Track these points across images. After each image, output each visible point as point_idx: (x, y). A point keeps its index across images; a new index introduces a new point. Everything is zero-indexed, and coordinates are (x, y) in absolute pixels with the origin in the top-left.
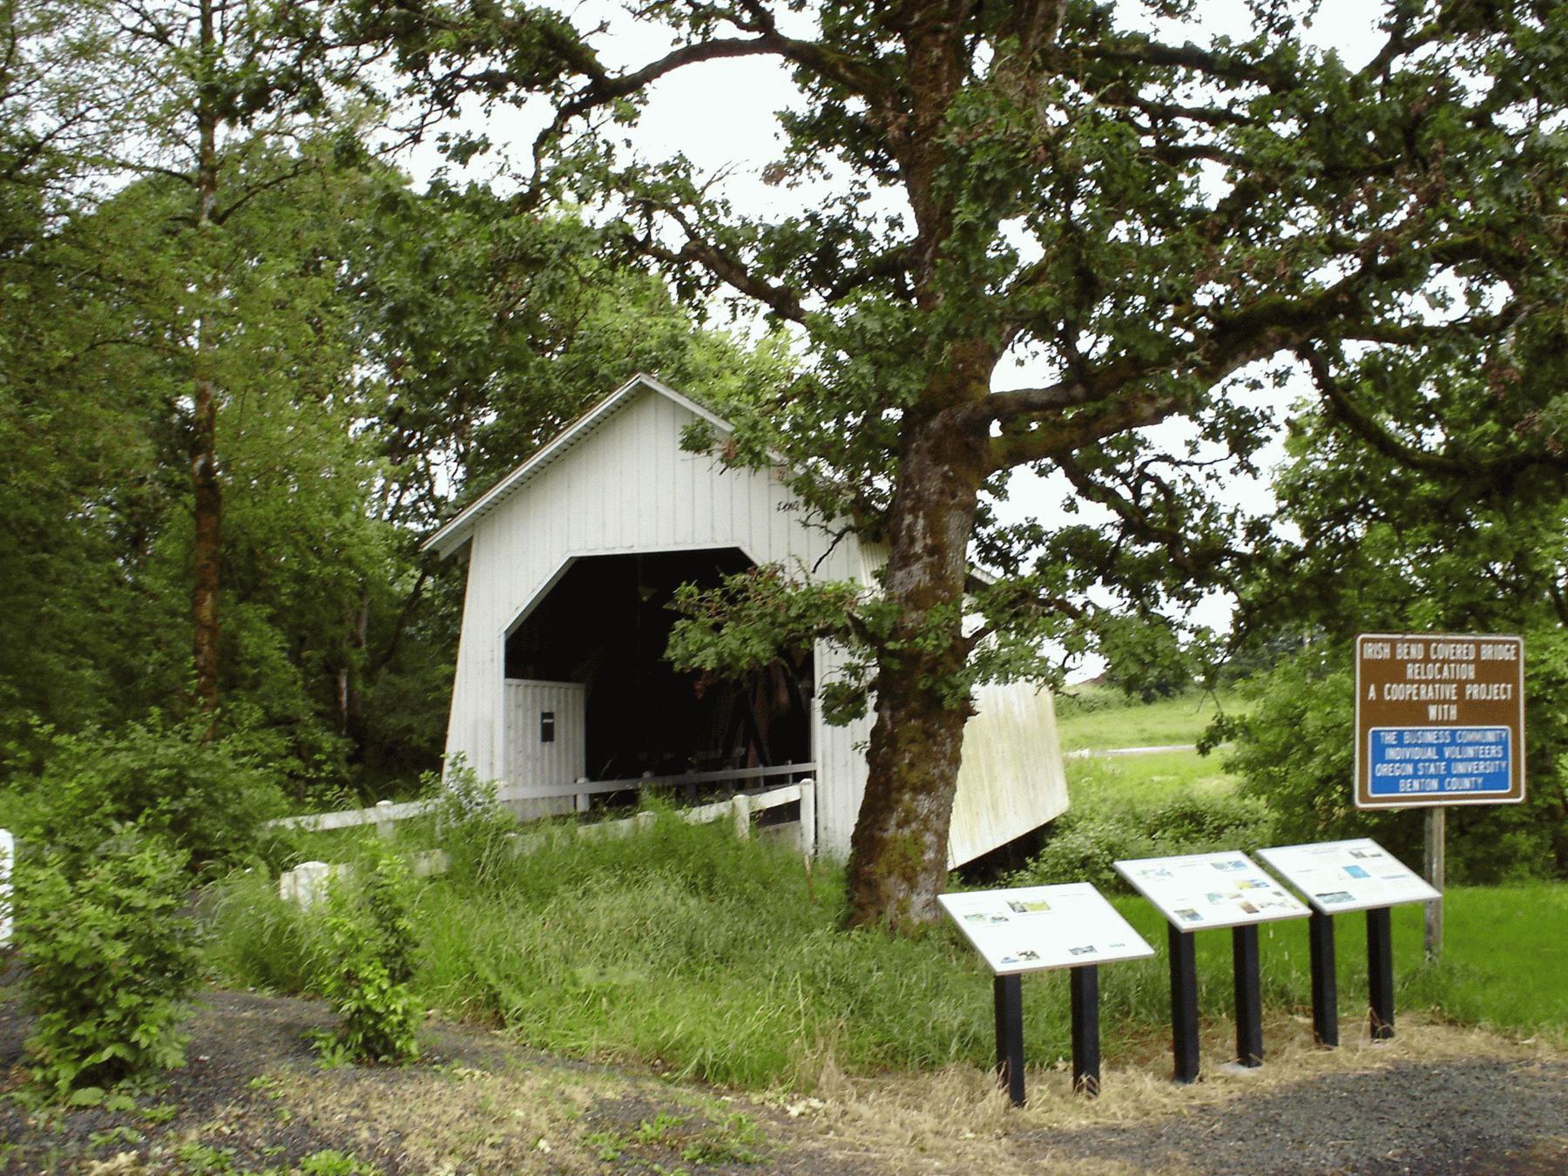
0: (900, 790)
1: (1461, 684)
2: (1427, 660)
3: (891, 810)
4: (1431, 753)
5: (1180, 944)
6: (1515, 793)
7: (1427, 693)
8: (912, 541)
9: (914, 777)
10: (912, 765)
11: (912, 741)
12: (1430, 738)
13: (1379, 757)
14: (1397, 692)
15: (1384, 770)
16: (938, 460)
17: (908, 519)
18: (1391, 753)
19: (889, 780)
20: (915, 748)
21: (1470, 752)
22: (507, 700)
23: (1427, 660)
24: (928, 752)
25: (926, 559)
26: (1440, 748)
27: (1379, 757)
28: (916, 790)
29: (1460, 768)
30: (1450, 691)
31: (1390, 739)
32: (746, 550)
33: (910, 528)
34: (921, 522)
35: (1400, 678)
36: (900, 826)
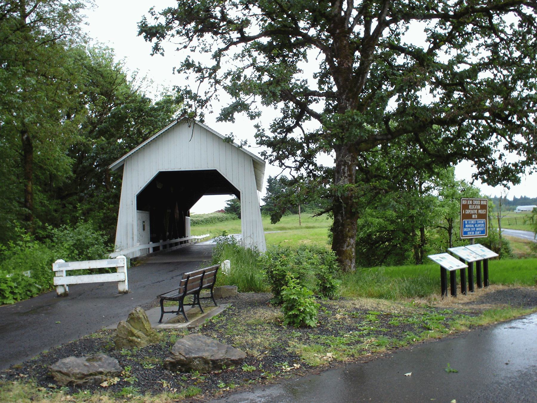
0: (346, 238)
1: (478, 210)
2: (472, 204)
3: (345, 243)
4: (473, 226)
5: (470, 264)
6: (486, 235)
7: (472, 212)
8: (344, 173)
9: (350, 234)
10: (349, 231)
11: (349, 225)
12: (473, 222)
13: (465, 227)
14: (468, 212)
15: (465, 230)
16: (350, 152)
17: (343, 167)
18: (467, 226)
19: (343, 235)
20: (349, 227)
21: (479, 225)
22: (139, 219)
23: (472, 204)
24: (352, 228)
25: (349, 178)
26: (474, 224)
27: (465, 227)
28: (350, 237)
29: (477, 229)
30: (476, 211)
31: (466, 222)
32: (222, 172)
33: (343, 169)
34: (346, 168)
35: (468, 209)
36: (347, 247)
